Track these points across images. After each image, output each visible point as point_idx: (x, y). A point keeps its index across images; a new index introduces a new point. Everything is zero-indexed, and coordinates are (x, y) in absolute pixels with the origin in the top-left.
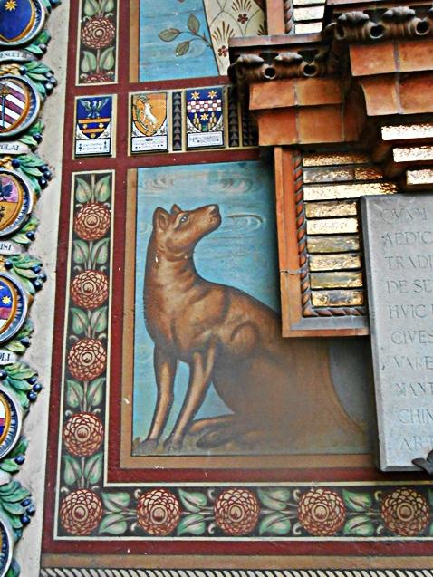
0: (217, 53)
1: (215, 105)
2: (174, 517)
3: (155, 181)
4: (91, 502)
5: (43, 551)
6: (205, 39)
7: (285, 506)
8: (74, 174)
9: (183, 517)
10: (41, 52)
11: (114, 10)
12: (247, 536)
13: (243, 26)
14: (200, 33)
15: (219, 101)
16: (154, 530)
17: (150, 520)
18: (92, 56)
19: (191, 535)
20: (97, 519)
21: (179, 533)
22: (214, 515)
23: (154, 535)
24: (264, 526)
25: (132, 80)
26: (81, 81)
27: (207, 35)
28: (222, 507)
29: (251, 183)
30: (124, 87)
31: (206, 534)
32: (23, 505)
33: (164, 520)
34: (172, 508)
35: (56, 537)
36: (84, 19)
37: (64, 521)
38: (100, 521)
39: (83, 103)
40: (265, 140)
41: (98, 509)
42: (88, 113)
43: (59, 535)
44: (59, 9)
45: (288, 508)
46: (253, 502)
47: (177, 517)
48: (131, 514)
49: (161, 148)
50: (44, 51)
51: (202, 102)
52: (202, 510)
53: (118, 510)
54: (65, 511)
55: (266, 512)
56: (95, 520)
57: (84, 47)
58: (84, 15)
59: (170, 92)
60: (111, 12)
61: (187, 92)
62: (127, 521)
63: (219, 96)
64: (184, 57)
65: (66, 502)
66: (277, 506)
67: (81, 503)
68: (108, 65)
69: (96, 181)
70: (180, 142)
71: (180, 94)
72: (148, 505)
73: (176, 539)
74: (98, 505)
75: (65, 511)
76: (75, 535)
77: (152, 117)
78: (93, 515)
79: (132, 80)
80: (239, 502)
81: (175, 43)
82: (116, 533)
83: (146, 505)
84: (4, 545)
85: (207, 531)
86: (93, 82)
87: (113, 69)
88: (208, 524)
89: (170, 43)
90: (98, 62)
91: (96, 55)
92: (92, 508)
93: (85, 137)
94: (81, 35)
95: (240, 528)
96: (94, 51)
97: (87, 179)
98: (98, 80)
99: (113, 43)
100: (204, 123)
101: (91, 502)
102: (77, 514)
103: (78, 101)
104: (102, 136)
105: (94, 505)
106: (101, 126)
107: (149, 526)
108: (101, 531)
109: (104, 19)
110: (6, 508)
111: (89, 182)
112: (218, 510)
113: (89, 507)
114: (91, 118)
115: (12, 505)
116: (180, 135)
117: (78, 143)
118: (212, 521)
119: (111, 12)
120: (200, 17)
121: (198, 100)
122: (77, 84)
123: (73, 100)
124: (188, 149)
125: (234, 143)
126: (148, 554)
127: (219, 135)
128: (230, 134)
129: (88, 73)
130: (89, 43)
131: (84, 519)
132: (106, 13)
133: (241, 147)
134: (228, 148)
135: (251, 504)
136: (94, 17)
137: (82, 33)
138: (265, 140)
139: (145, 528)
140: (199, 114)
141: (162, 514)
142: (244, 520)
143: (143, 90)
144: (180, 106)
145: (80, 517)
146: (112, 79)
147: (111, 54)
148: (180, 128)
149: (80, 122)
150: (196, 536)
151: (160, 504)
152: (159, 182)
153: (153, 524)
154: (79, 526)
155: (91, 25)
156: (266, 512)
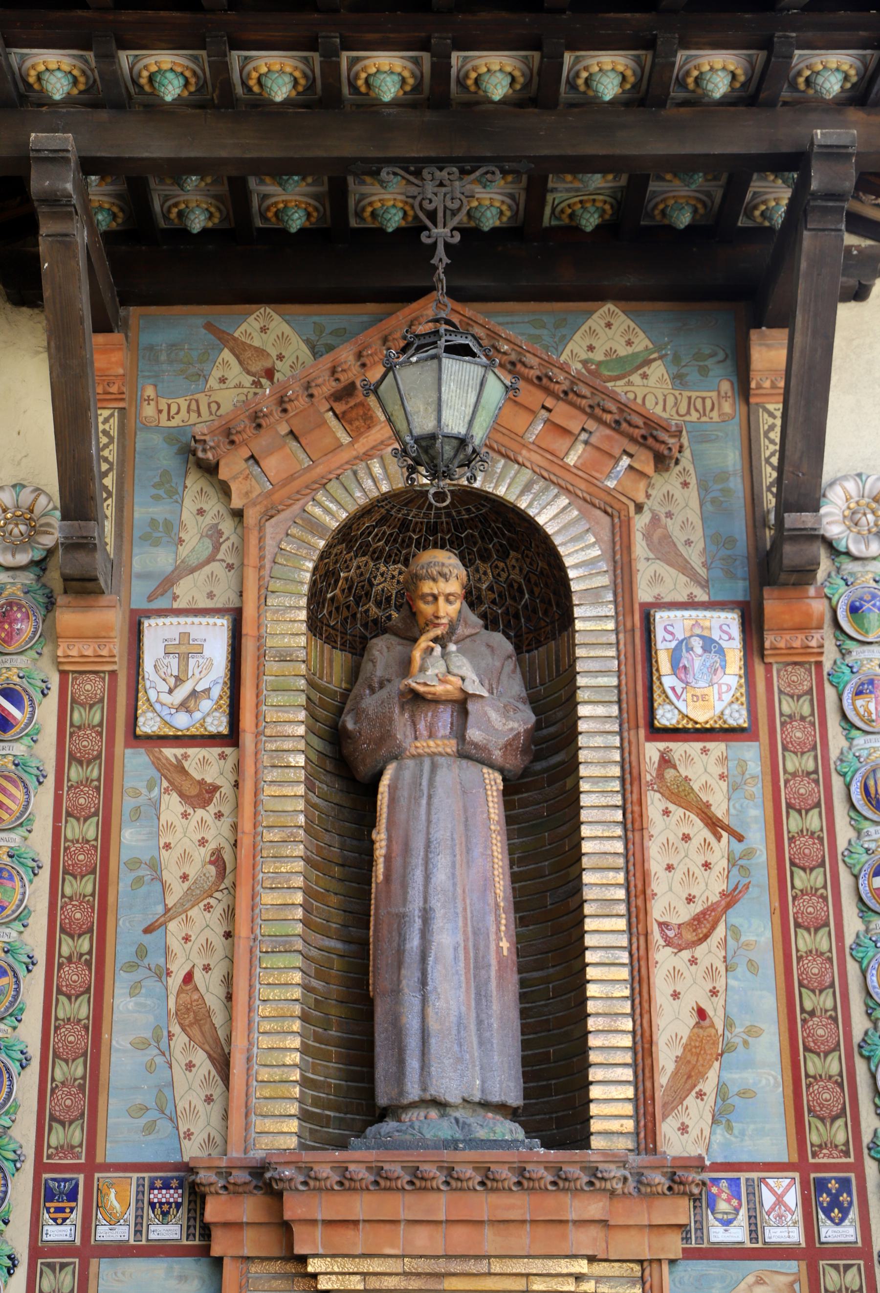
0: (182, 1136)
1: (176, 1196)
3: (116, 1274)
6: (171, 1119)
8: (40, 1261)
11: (84, 1078)
13: (209, 1107)
14: (167, 1112)
15: (180, 1191)
18: (60, 1128)
25: (99, 1159)
26: (49, 1157)
27: (174, 1115)
29: (204, 1281)
30: (91, 1167)
39: (51, 1183)
40: (216, 1251)
42: (55, 1195)
44: (28, 1070)
49: (123, 1238)
50: (13, 1121)
51: (164, 1191)
57: (53, 1118)
58: (53, 1080)
59: (135, 1176)
61: (150, 1178)
63: (181, 1186)
64: (151, 1137)
68: (76, 1141)
69: (61, 1270)
70: (141, 1232)
71: (144, 1178)
77: (115, 1203)
79: (99, 1159)
81: (142, 1121)
86: (60, 1158)
87: (81, 1145)
89: (137, 1121)
90: (66, 1136)
93: (51, 1222)
96: (62, 1124)
97: (51, 1266)
98: (66, 1158)
99: (82, 1114)
100: (165, 1214)
103: (46, 1180)
104: (68, 1221)
106: (68, 1210)
109: (73, 1086)
111: (54, 1271)
114: (58, 1201)
116: (142, 1224)
117: (45, 1228)
120: (167, 1092)
121: (161, 1188)
122: (45, 1161)
123: (40, 1178)
124: (148, 1240)
125: (191, 1237)
127: (178, 1227)
128: (189, 1227)
129: (56, 1148)
132: (75, 1080)
133: (197, 1242)
134: (185, 1242)
136: (63, 1083)
138: (216, 1251)
140: (161, 1204)
143: (109, 1171)
144: (143, 1193)
146: (79, 1158)
148: (142, 1217)
149: (48, 1205)
152: (119, 1275)
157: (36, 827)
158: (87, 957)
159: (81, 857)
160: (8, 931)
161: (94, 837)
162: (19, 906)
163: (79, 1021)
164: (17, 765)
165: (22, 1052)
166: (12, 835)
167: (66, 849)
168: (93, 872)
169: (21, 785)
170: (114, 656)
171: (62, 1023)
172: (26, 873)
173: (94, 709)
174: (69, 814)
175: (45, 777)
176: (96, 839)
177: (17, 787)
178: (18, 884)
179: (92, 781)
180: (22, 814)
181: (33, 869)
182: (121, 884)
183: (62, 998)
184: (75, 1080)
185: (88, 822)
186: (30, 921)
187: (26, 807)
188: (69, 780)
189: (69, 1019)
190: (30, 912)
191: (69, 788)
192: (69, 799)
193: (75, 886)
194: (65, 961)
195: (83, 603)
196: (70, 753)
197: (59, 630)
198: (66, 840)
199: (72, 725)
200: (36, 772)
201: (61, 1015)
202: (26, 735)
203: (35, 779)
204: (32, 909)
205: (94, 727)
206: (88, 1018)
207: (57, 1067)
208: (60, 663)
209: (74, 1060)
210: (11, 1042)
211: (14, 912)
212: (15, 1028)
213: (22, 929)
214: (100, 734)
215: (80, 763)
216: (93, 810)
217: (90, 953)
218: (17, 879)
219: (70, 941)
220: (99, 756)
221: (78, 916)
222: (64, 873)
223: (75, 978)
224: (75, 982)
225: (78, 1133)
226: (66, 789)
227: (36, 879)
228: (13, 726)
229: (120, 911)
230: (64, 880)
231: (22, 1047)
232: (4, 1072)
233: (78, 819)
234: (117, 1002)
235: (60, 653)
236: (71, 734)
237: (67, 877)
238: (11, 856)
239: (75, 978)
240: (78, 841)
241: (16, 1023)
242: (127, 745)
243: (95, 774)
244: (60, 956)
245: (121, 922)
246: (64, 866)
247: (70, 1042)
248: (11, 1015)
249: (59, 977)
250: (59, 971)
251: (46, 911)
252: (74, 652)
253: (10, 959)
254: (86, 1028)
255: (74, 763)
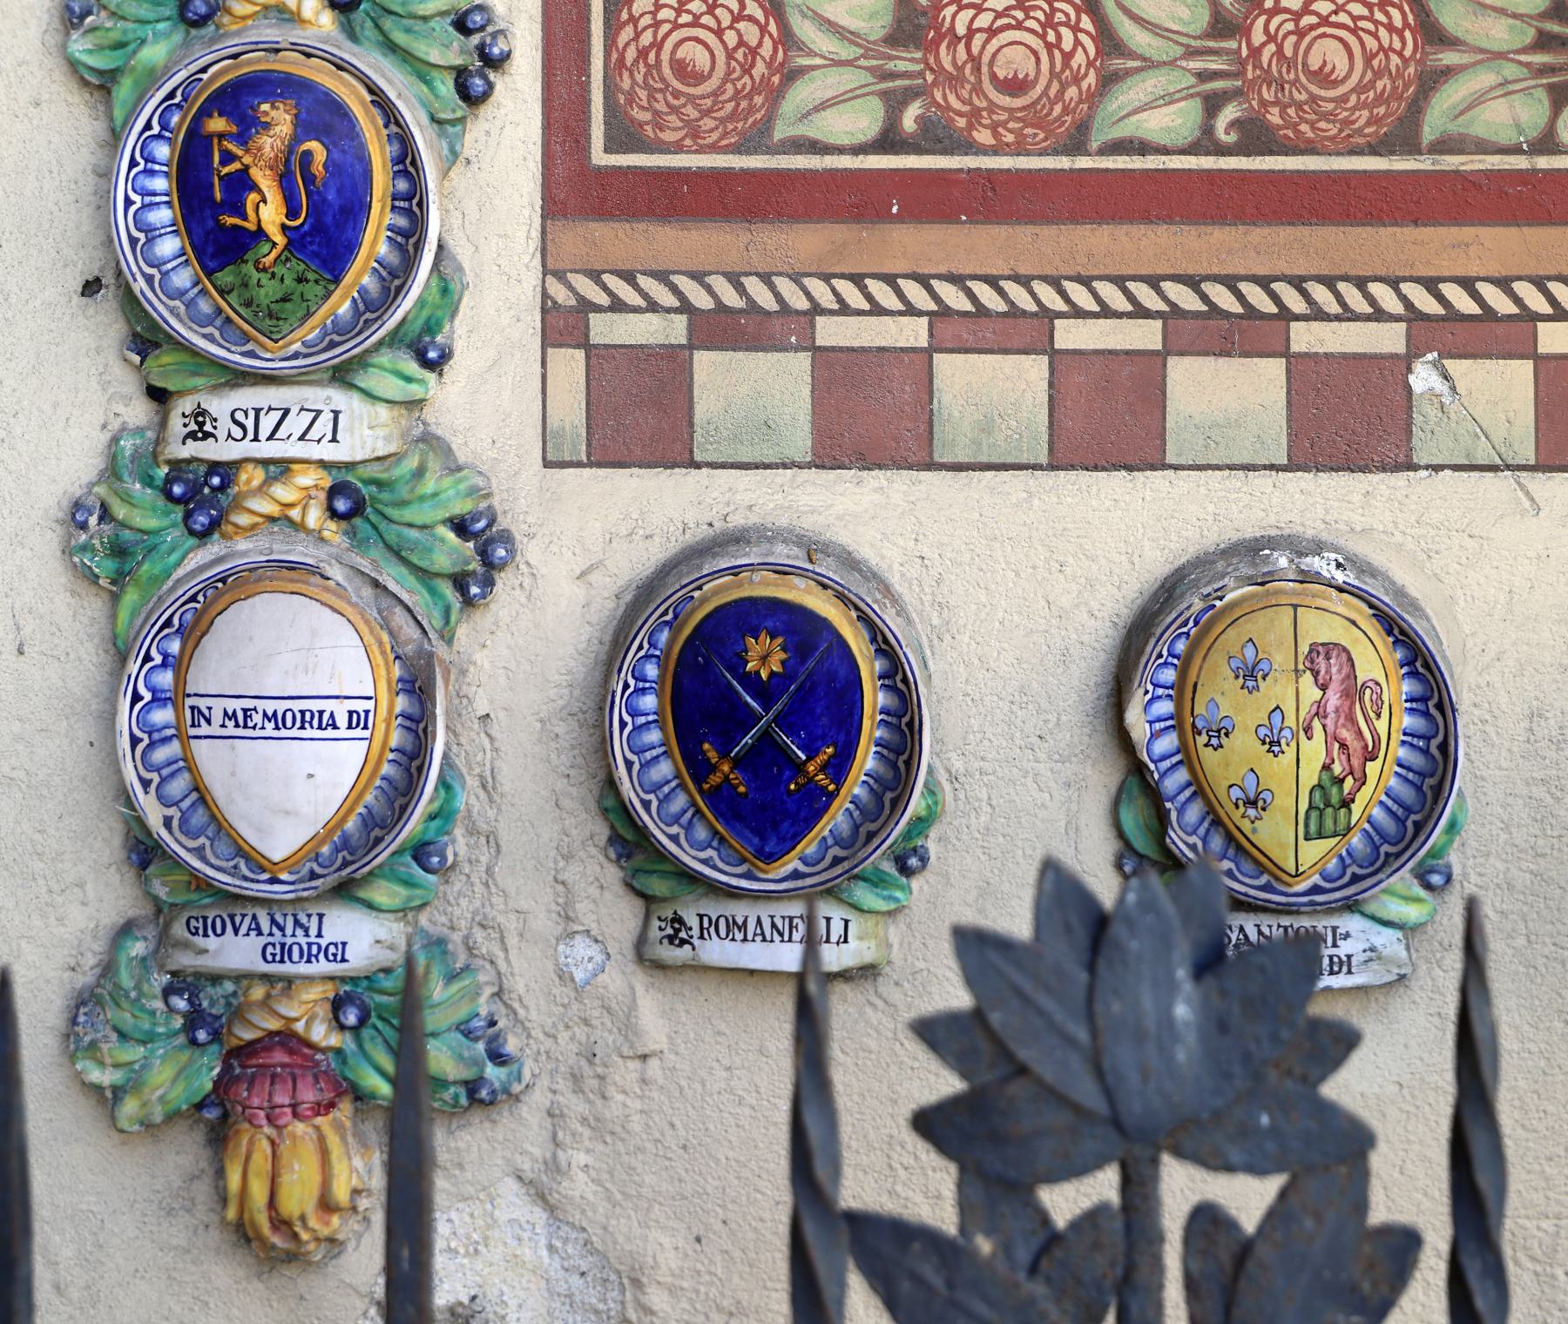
2: (1077, 80)
4: (737, 19)
5: (555, 206)
7: (1530, 35)
9: (1109, 80)
12: (1373, 151)
16: (994, 128)
17: (978, 89)
19: (1143, 148)
20: (763, 85)
21: (1095, 145)
22: (1240, 74)
23: (995, 151)
24: (1434, 123)
28: (1271, 38)
31: (1205, 143)
32: (462, 25)
33: (1039, 89)
34: (1068, 43)
35: (600, 157)
37: (631, 98)
38: (776, 96)
41: (767, 49)
43: (607, 150)
45: (1544, 42)
46: (1398, 21)
47: (1091, 79)
48: (902, 66)
52: (1191, 53)
53: (846, 52)
54: (631, 54)
55: (1449, 58)
56: (755, 90)
62: (884, 95)
65: (633, 20)
66: (1499, 34)
67: (695, 23)
72: (971, 32)
73: (1083, 162)
74: (763, 29)
75: (631, 54)
76: (678, 148)
78: (747, 71)
80: (1343, 18)
82: (845, 141)
83: (961, 30)
84: (402, 185)
85: (1208, 130)
88: (1212, 104)
92: (741, 43)
95: (1347, 122)
101: (737, 19)
102: (682, 69)
105: (751, 33)
107: (974, 115)
108: (781, 132)
110: (400, 37)
112: (1256, 52)
113: (731, 38)
115: (418, 26)
118: (1237, 93)
126: (970, 221)
131: (707, 87)
135: (1390, 28)
139: (961, 122)
141: (1026, 67)
142: (1360, 89)
145: (699, 78)
150: (1165, 151)
151: (1019, 26)
153: (992, 107)
154: (694, 114)
156: (1449, 58)
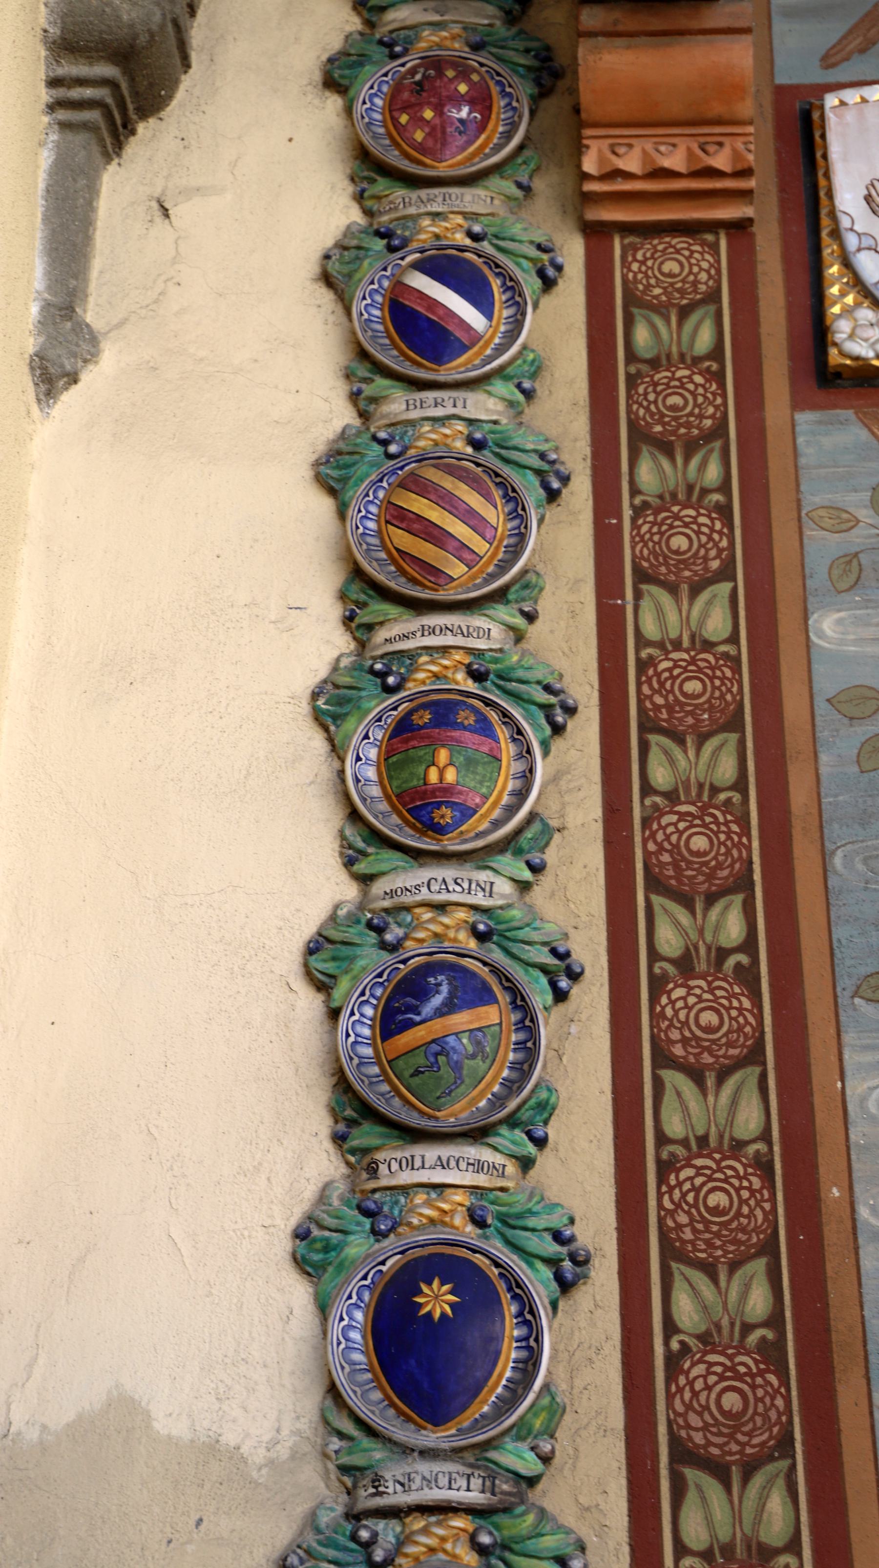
10: (539, 1467)
11: (775, 1320)
18: (713, 1488)
36: (675, 1345)
44: (583, 1296)
50: (546, 1459)
58: (670, 1327)
60: (765, 1324)
90: (737, 1516)
91: (727, 1487)
94: (670, 1404)
99: (785, 1443)
109: (742, 1348)
119: (765, 1324)
130: (698, 1438)
132: (747, 1328)
136: (704, 1338)
137: (670, 1397)
147: (781, 1482)
155: (700, 1369)
157: (546, 606)
158: (744, 959)
159: (693, 686)
160: (484, 876)
161: (726, 634)
162: (511, 810)
163: (738, 1145)
164: (478, 445)
165: (558, 1237)
166: (478, 621)
167: (642, 666)
168: (735, 724)
169: (497, 494)
170: (745, 173)
171: (680, 1151)
172: (529, 717)
173: (694, 318)
174: (642, 576)
175: (565, 480)
176: (734, 639)
177: (487, 496)
178: (508, 750)
179: (705, 492)
180: (504, 567)
181: (546, 708)
182: (824, 758)
183: (673, 1078)
184: (747, 1328)
185: (704, 596)
186: (551, 856)
187: (516, 551)
188: (635, 491)
189: (703, 1140)
190: (548, 833)
191: (638, 511)
192: (638, 538)
193: (682, 763)
194: (671, 969)
195: (656, 24)
196: (632, 425)
197: (586, 98)
198: (641, 641)
199: (631, 356)
200: (534, 461)
201: (675, 1127)
202: (499, 372)
203: (534, 480)
204: (554, 823)
205: (696, 360)
206: (765, 1136)
207: (679, 1285)
208: (588, 198)
209: (734, 1267)
210: (519, 1201)
211: (497, 824)
212: (526, 1164)
213: (527, 875)
214: (719, 377)
215: (666, 448)
216: (715, 564)
217: (749, 945)
218: (503, 733)
219: (683, 917)
220: (720, 430)
221: (700, 843)
222: (643, 729)
223: (710, 1018)
224: (709, 1029)
225: (777, 1503)
226: (627, 513)
227: (558, 745)
228: (465, 348)
229: (834, 831)
230: (644, 748)
231: (556, 1221)
232: (505, 1297)
233: (673, 589)
234: (855, 1088)
235: (589, 165)
236: (632, 381)
237: (653, 738)
238: (478, 676)
239: (710, 1018)
240: (677, 645)
241: (531, 1149)
242: (798, 404)
243: (713, 473)
244: (654, 955)
245: (838, 861)
246: (641, 710)
247: (716, 1211)
248: (512, 1121)
249: (656, 1017)
250: (654, 1000)
251: (597, 830)
252: (631, 163)
253: (497, 956)
254: (764, 1167)
255: (645, 451)
